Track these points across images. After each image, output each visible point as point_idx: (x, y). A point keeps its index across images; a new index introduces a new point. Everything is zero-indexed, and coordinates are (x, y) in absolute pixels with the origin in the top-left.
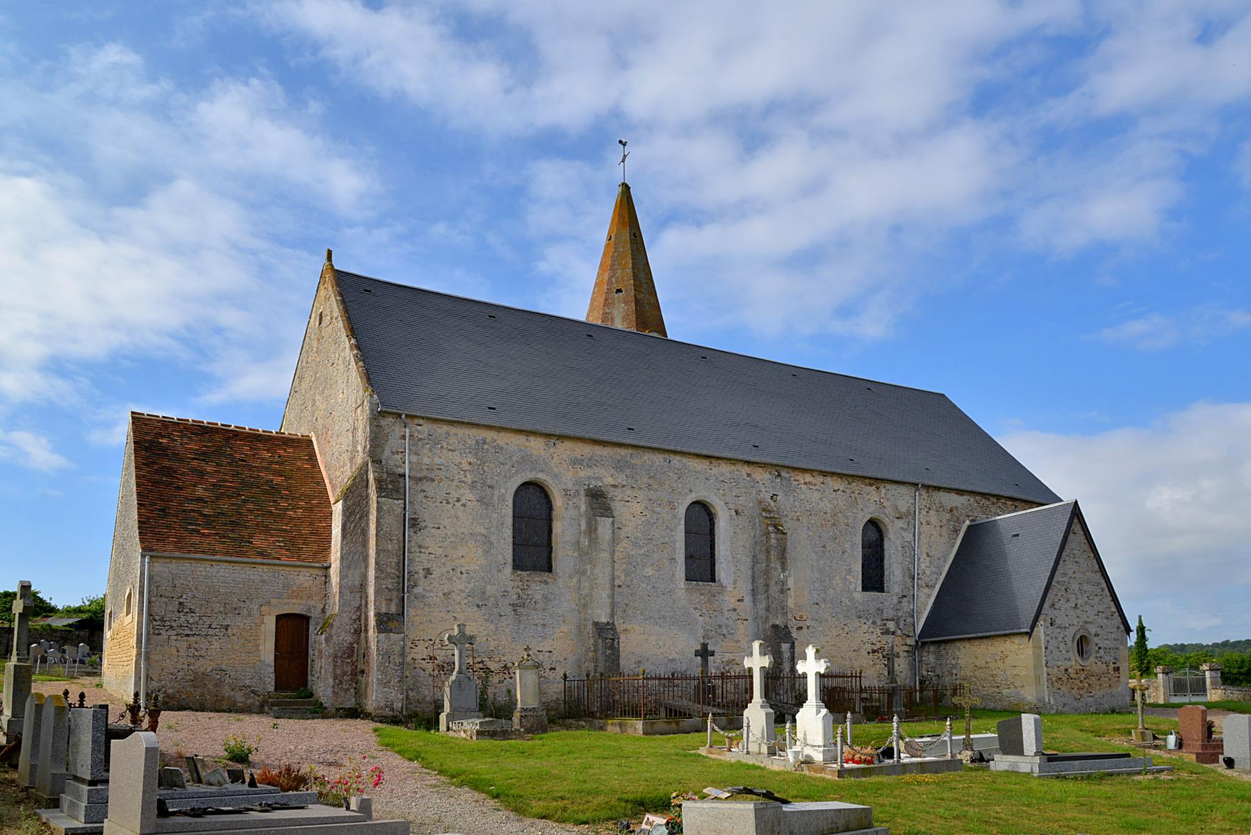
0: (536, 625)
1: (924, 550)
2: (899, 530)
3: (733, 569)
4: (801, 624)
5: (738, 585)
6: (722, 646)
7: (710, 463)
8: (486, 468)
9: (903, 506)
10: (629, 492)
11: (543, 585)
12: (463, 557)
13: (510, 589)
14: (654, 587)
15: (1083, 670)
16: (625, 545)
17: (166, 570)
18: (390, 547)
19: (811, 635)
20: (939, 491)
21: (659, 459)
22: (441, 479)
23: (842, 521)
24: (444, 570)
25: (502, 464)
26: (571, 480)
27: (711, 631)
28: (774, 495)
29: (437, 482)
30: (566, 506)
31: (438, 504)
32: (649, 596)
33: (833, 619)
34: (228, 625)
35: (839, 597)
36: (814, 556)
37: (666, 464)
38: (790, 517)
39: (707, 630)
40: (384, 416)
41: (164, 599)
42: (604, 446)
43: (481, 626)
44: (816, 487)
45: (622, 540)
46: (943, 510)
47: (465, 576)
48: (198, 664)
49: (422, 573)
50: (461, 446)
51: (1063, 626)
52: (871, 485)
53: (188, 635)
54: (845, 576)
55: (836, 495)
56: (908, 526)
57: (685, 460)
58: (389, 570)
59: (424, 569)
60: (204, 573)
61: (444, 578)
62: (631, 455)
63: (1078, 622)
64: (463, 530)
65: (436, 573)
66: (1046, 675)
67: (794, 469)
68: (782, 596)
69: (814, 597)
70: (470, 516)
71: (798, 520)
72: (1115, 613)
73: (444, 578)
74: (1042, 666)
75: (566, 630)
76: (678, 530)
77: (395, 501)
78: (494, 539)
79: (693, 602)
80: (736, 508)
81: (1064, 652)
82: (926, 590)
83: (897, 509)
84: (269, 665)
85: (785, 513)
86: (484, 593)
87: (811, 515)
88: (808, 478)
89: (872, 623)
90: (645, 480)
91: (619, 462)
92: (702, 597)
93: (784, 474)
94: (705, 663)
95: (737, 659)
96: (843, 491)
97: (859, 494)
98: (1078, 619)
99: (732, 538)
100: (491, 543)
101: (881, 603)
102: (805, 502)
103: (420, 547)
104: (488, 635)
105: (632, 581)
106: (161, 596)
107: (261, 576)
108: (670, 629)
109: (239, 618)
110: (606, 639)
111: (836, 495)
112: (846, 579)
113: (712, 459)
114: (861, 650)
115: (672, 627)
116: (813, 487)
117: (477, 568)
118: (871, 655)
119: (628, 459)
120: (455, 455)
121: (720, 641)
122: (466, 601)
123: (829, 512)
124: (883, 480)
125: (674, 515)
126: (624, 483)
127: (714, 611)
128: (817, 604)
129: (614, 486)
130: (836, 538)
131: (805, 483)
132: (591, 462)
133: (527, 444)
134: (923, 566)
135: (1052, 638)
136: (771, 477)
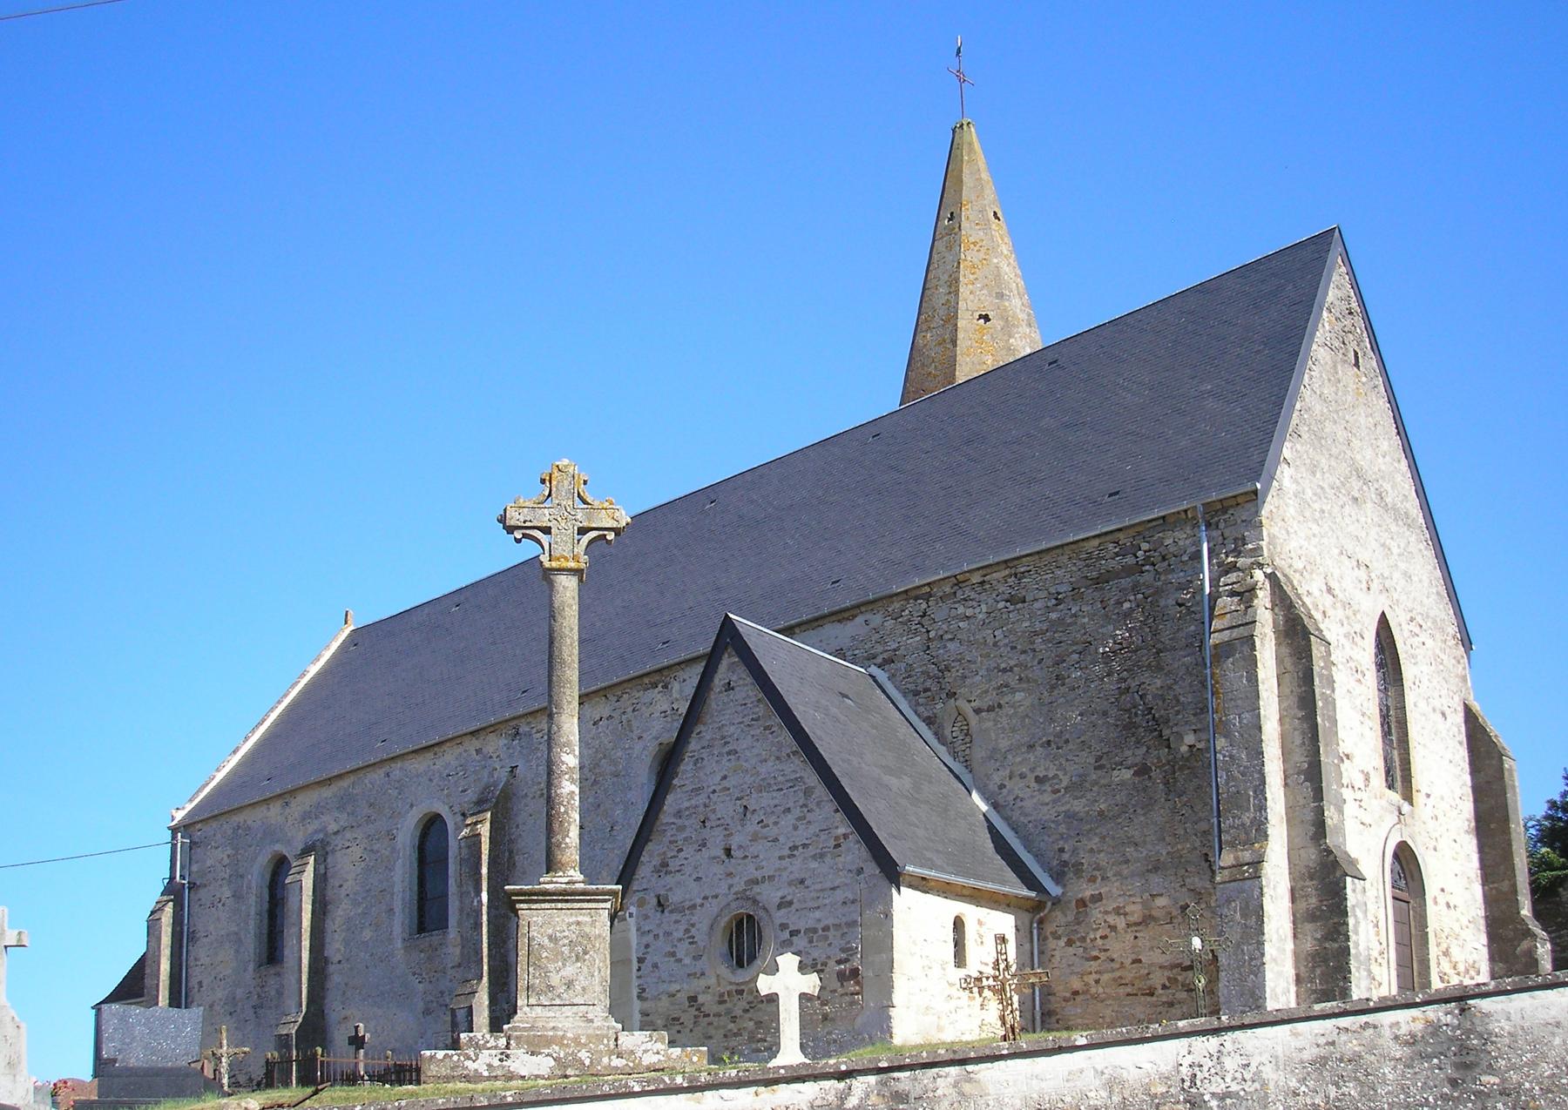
7: (435, 754)
27: (432, 1001)
38: (531, 796)
47: (223, 982)
51: (687, 904)
72: (845, 836)
81: (687, 961)
86: (234, 998)
92: (422, 955)
93: (524, 729)
97: (634, 710)
127: (436, 972)
135: (656, 936)
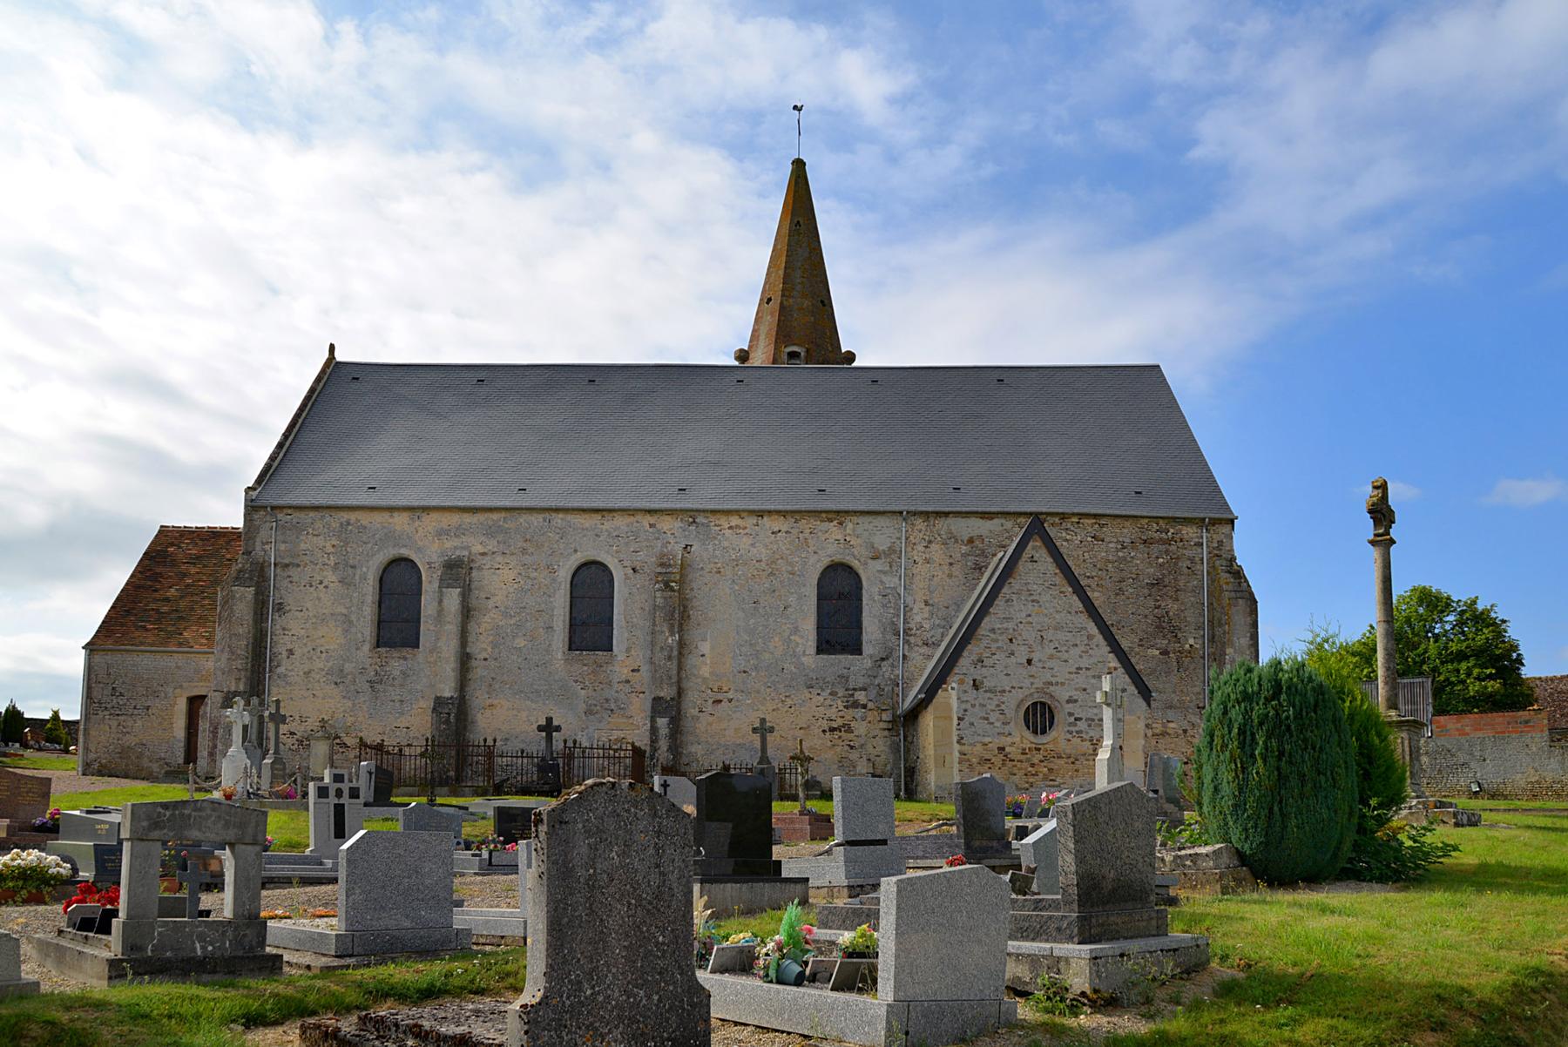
0: (394, 701)
1: (920, 596)
2: (877, 574)
3: (626, 635)
4: (720, 697)
5: (633, 652)
6: (609, 723)
7: (603, 516)
8: (349, 549)
9: (882, 543)
10: (499, 558)
11: (401, 661)
12: (323, 637)
13: (368, 666)
14: (526, 659)
15: (1039, 749)
16: (492, 615)
17: (104, 661)
18: (241, 631)
19: (734, 709)
20: (946, 517)
21: (536, 520)
22: (306, 564)
23: (784, 569)
24: (306, 650)
25: (365, 543)
26: (436, 552)
27: (596, 705)
28: (687, 545)
29: (302, 567)
30: (430, 579)
31: (302, 588)
32: (519, 668)
33: (768, 690)
34: (149, 706)
35: (779, 663)
36: (741, 614)
37: (546, 524)
38: (708, 570)
39: (591, 705)
40: (256, 511)
41: (101, 685)
42: (474, 513)
43: (339, 702)
44: (746, 531)
45: (490, 610)
46: (956, 541)
47: (324, 655)
48: (125, 739)
49: (285, 654)
50: (326, 530)
51: (999, 689)
52: (831, 520)
53: (118, 715)
54: (789, 637)
55: (776, 537)
56: (891, 567)
57: (569, 517)
58: (239, 652)
59: (287, 650)
60: (132, 662)
61: (305, 657)
62: (504, 518)
63: (1032, 684)
64: (325, 611)
65: (298, 653)
66: (957, 754)
67: (714, 512)
68: (669, 663)
69: (740, 664)
70: (332, 598)
71: (720, 572)
72: (1115, 669)
73: (305, 657)
74: (952, 743)
75: (425, 706)
76: (556, 596)
77: (247, 589)
78: (353, 618)
79: (574, 674)
80: (633, 566)
81: (998, 724)
82: (924, 650)
83: (873, 547)
84: (179, 741)
85: (701, 565)
86: (342, 671)
87: (737, 565)
88: (735, 521)
89: (830, 694)
90: (520, 544)
91: (490, 527)
92: (585, 668)
93: (700, 519)
94: (549, 739)
95: (628, 737)
96: (787, 532)
97: (811, 533)
98: (1032, 680)
99: (627, 600)
100: (351, 622)
101: (845, 668)
102: (731, 551)
103: (284, 629)
104: (345, 711)
105: (500, 653)
106: (99, 682)
107: (176, 663)
108: (544, 704)
109: (157, 700)
110: (441, 713)
111: (776, 537)
112: (791, 640)
113: (604, 513)
114: (812, 727)
115: (547, 702)
116: (741, 531)
117: (336, 646)
118: (828, 734)
119: (501, 523)
120: (320, 541)
121: (606, 717)
122: (325, 679)
123: (764, 559)
124: (847, 512)
125: (553, 580)
126: (495, 550)
127: (600, 683)
128: (745, 672)
129: (483, 554)
130: (774, 591)
131: (730, 528)
132: (459, 531)
133: (390, 520)
134: (918, 619)
135: (973, 706)
136: (682, 525)
